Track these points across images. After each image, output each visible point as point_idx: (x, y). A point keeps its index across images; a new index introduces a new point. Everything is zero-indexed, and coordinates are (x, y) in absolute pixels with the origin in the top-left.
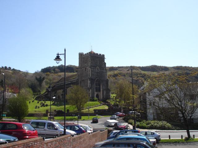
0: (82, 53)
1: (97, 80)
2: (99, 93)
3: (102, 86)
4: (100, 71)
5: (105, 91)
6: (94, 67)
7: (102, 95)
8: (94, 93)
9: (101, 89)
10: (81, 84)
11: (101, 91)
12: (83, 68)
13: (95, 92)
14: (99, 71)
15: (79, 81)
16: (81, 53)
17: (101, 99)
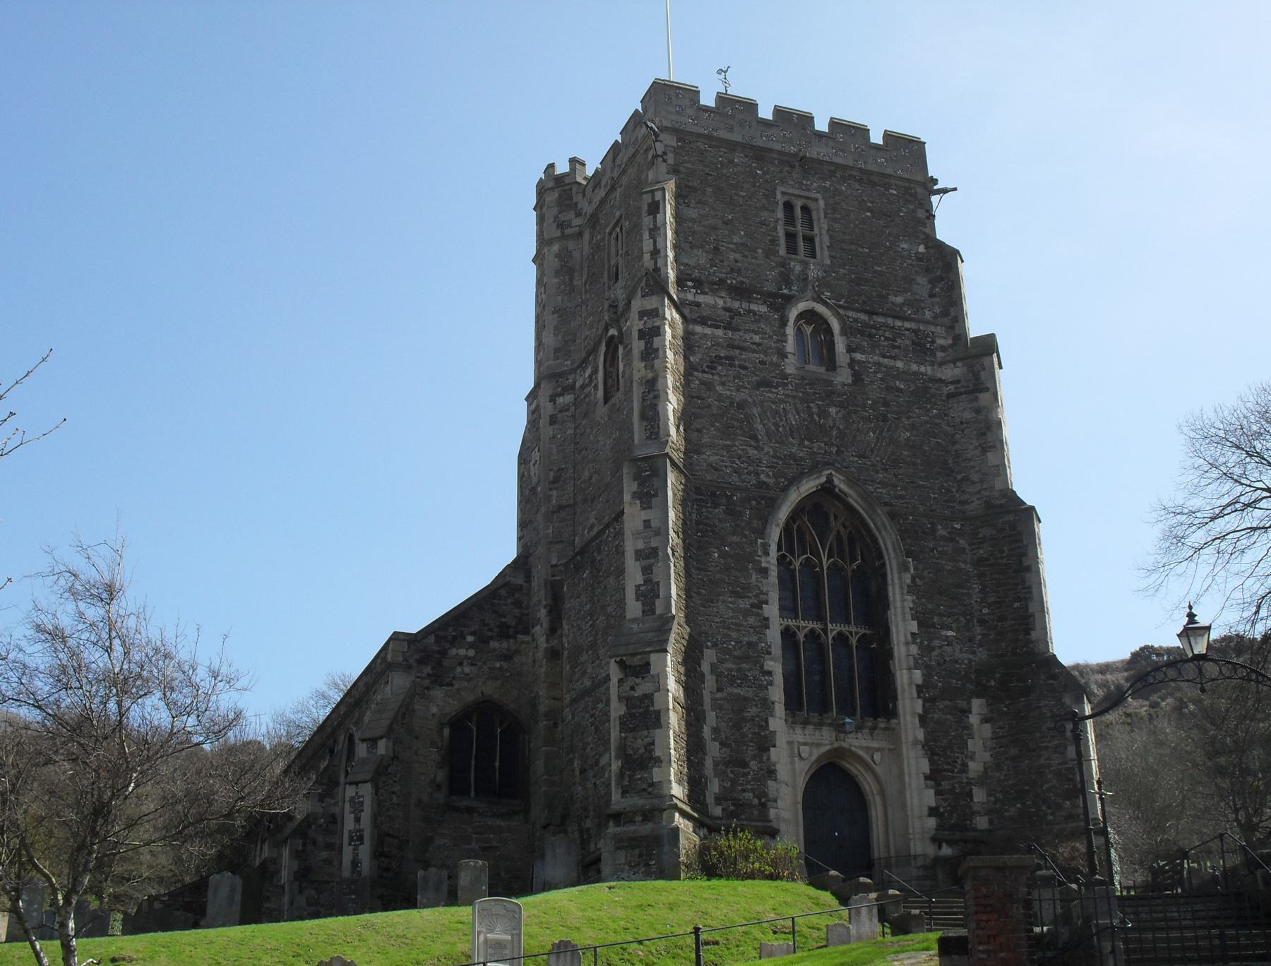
0: (574, 161)
1: (814, 508)
2: (857, 742)
3: (924, 621)
4: (857, 378)
5: (977, 705)
6: (740, 292)
7: (933, 777)
8: (765, 743)
9: (906, 678)
10: (553, 630)
11: (909, 706)
12: (583, 364)
13: (777, 723)
14: (843, 377)
15: (540, 573)
16: (562, 168)
17: (922, 847)
